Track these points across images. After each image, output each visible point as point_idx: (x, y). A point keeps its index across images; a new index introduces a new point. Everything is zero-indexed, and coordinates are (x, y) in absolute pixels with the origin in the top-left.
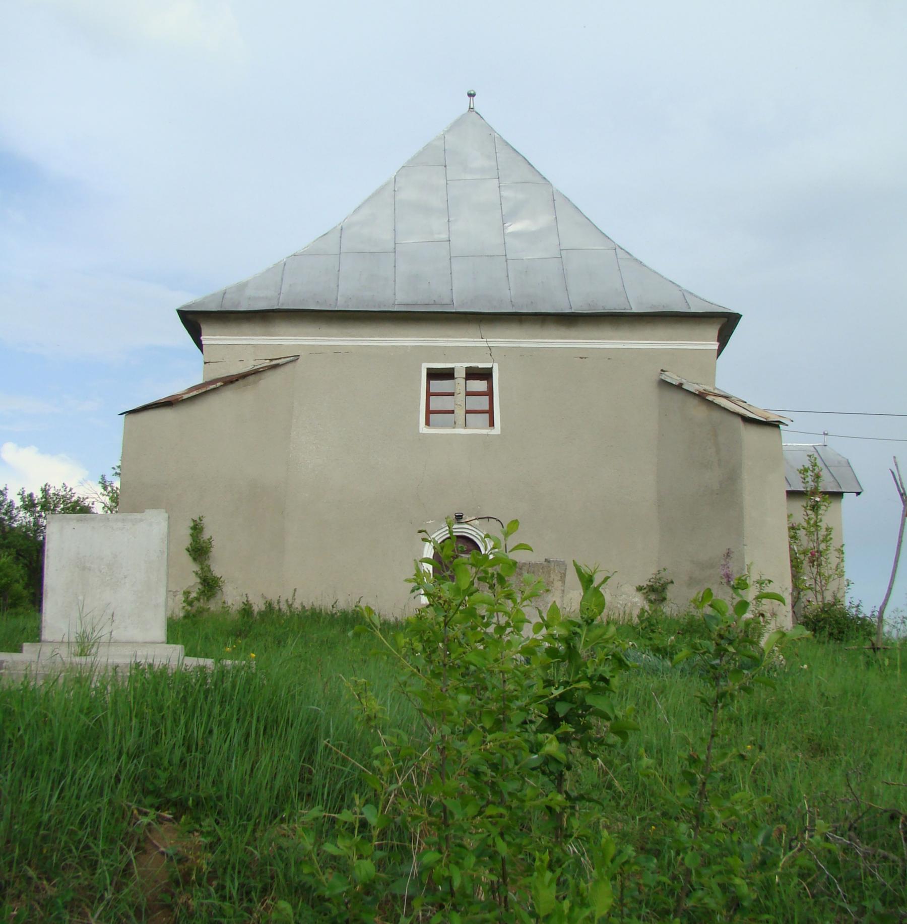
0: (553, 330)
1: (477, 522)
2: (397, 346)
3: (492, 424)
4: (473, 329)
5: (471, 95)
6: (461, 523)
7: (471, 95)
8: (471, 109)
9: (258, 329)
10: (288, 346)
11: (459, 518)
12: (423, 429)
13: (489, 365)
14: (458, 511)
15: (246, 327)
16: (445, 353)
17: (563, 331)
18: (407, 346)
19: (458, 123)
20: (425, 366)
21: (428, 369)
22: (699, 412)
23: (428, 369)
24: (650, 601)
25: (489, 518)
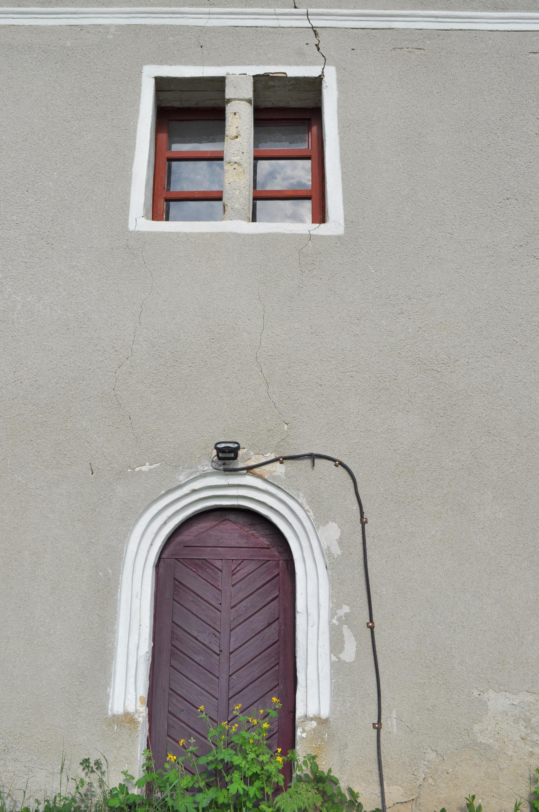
1: (279, 469)
2: (82, 28)
3: (320, 215)
6: (235, 471)
12: (138, 219)
13: (312, 72)
16: (201, 41)
18: (107, 27)
20: (150, 73)
21: (162, 85)
23: (162, 85)
25: (313, 457)
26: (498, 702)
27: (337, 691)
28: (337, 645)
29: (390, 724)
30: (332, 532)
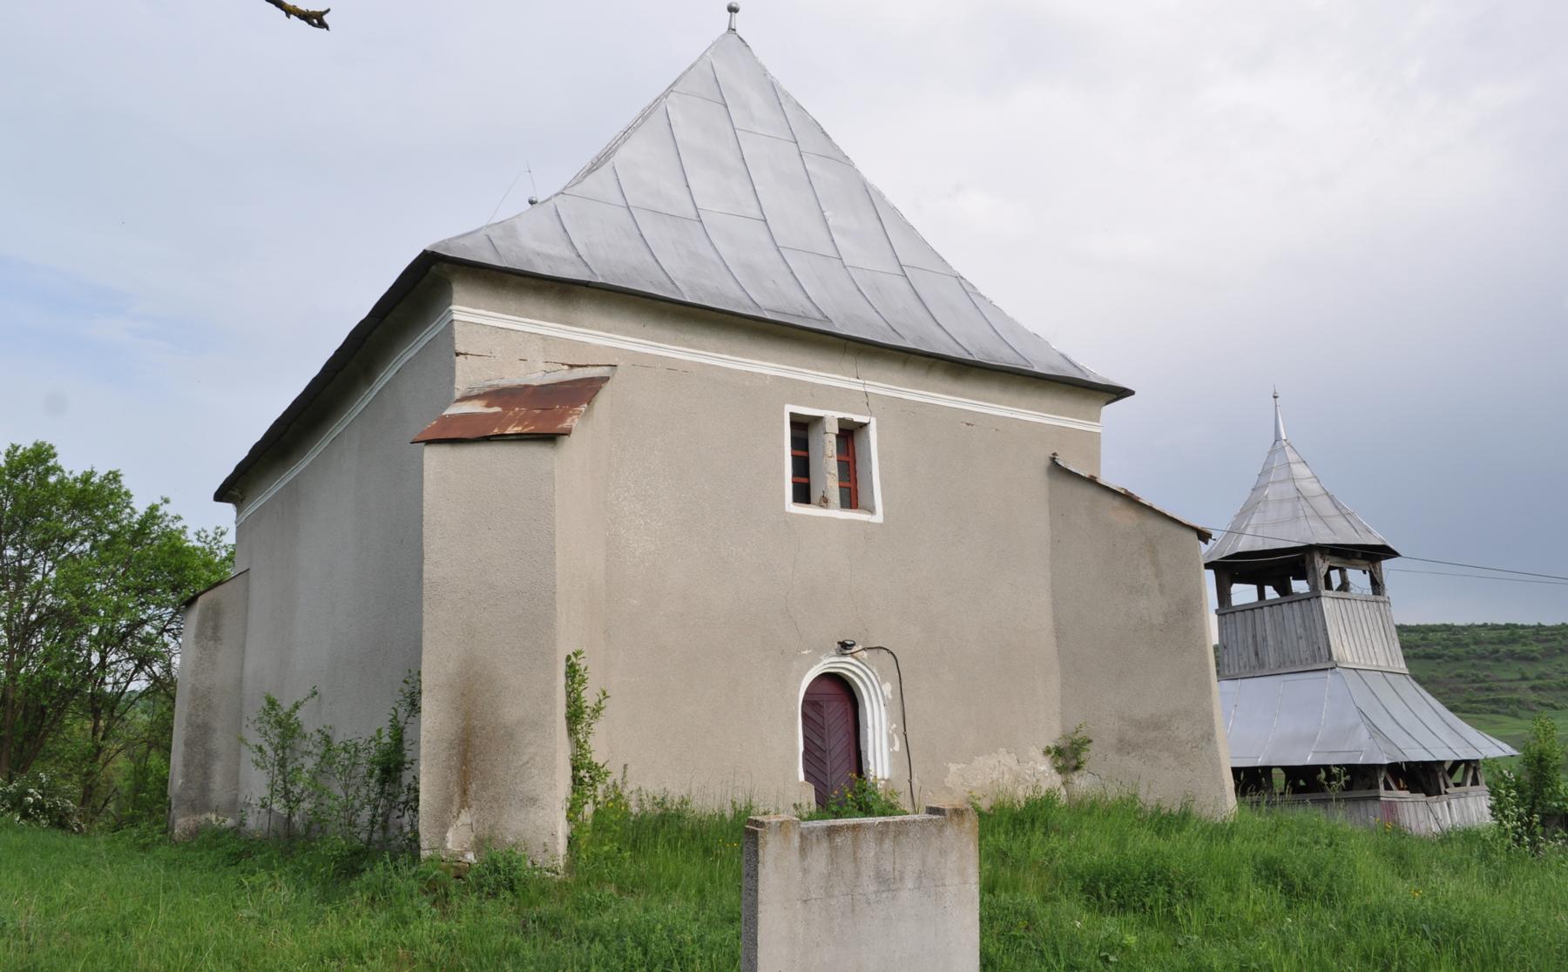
0: (937, 379)
1: (865, 654)
4: (848, 363)
5: (733, 10)
7: (733, 10)
8: (732, 30)
9: (550, 309)
10: (598, 347)
11: (845, 646)
14: (848, 639)
15: (531, 303)
17: (949, 383)
19: (717, 46)
21: (792, 414)
22: (1126, 518)
23: (792, 414)
24: (1060, 770)
26: (953, 767)
27: (892, 765)
28: (891, 743)
29: (915, 780)
30: (887, 688)
